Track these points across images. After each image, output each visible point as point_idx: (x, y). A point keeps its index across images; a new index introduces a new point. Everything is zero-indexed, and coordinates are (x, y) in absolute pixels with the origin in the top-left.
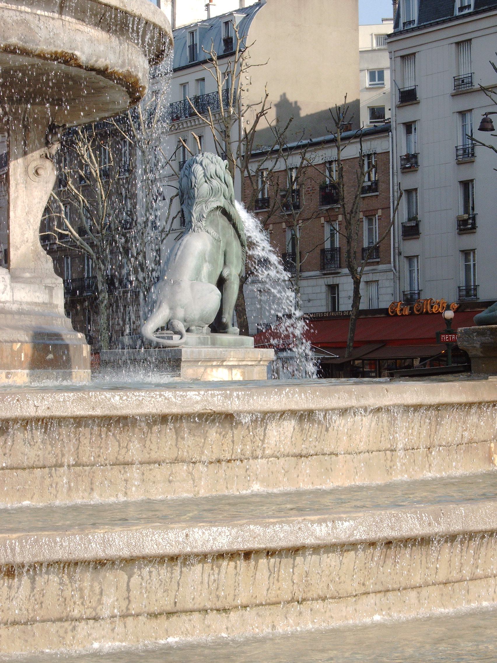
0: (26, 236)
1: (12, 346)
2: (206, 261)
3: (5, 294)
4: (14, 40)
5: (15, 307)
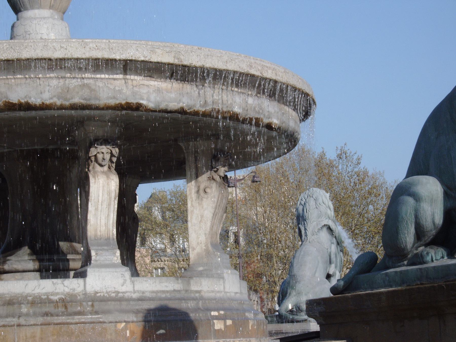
0: (200, 239)
1: (116, 326)
3: (124, 286)
4: (77, 100)
5: (135, 296)
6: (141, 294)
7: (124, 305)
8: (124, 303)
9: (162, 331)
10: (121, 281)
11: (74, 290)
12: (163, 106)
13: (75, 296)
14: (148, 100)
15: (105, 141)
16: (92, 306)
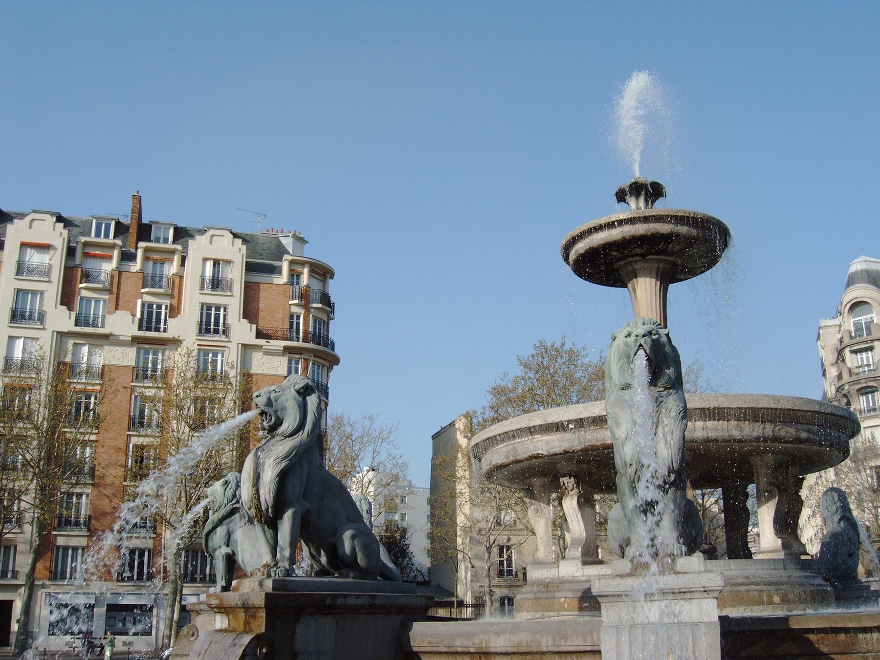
5: (584, 579)
6: (587, 578)
7: (574, 586)
8: (578, 584)
9: (586, 604)
10: (576, 568)
11: (554, 575)
12: (552, 452)
13: (554, 579)
14: (542, 450)
15: (564, 476)
16: (558, 586)
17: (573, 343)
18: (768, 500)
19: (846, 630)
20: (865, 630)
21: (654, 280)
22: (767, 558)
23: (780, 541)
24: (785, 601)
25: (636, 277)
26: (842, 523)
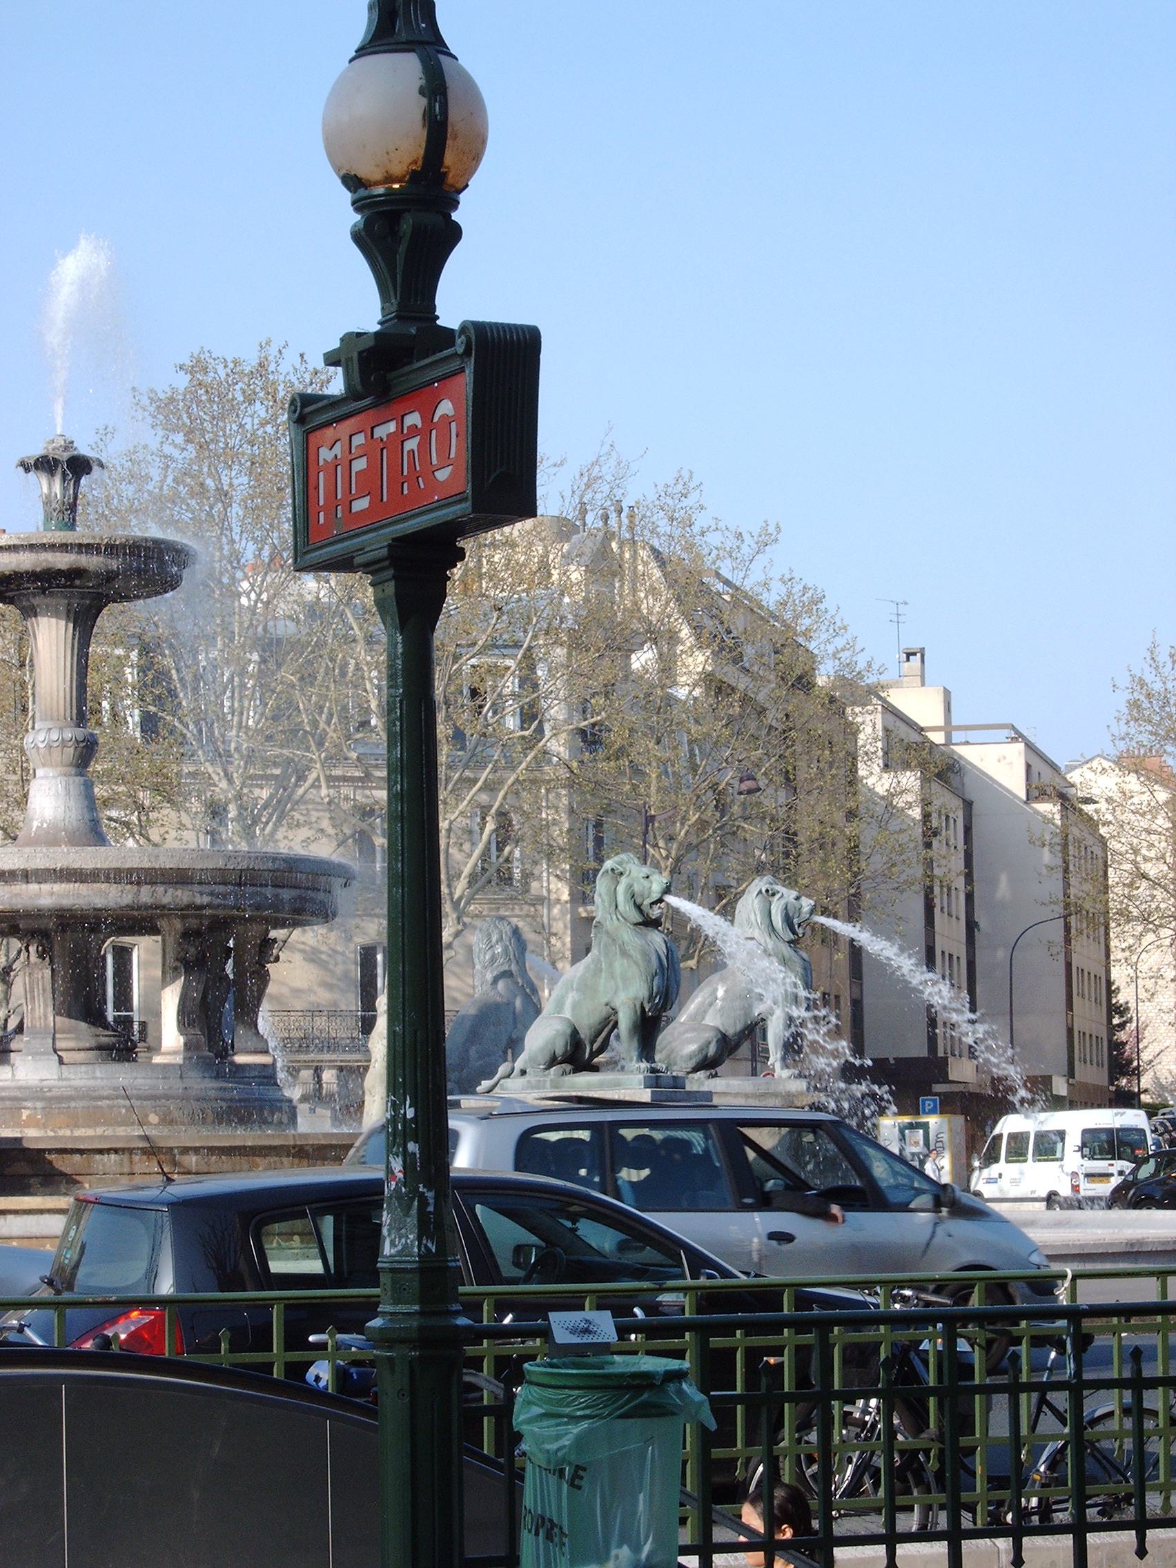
2: (572, 989)
17: (302, 356)
18: (173, 980)
19: (81, 1152)
20: (101, 1151)
21: (63, 623)
22: (165, 1061)
23: (182, 1040)
24: (167, 1120)
25: (36, 616)
26: (501, 985)
